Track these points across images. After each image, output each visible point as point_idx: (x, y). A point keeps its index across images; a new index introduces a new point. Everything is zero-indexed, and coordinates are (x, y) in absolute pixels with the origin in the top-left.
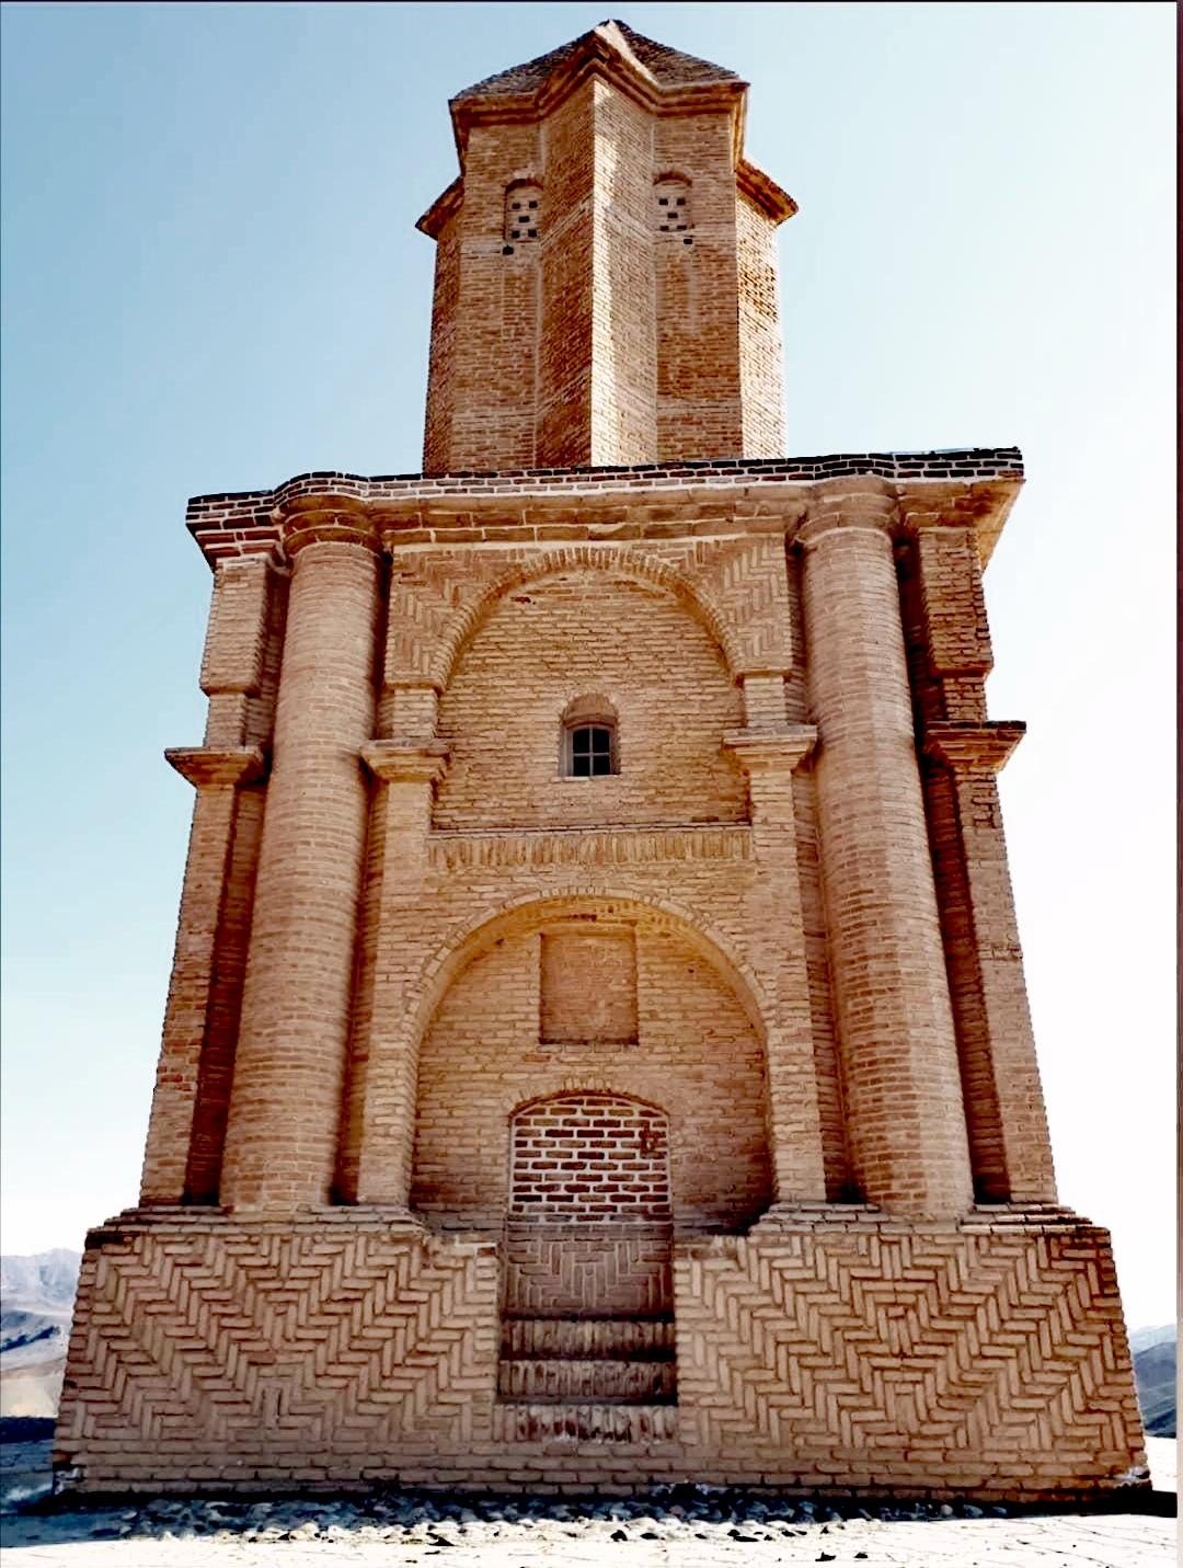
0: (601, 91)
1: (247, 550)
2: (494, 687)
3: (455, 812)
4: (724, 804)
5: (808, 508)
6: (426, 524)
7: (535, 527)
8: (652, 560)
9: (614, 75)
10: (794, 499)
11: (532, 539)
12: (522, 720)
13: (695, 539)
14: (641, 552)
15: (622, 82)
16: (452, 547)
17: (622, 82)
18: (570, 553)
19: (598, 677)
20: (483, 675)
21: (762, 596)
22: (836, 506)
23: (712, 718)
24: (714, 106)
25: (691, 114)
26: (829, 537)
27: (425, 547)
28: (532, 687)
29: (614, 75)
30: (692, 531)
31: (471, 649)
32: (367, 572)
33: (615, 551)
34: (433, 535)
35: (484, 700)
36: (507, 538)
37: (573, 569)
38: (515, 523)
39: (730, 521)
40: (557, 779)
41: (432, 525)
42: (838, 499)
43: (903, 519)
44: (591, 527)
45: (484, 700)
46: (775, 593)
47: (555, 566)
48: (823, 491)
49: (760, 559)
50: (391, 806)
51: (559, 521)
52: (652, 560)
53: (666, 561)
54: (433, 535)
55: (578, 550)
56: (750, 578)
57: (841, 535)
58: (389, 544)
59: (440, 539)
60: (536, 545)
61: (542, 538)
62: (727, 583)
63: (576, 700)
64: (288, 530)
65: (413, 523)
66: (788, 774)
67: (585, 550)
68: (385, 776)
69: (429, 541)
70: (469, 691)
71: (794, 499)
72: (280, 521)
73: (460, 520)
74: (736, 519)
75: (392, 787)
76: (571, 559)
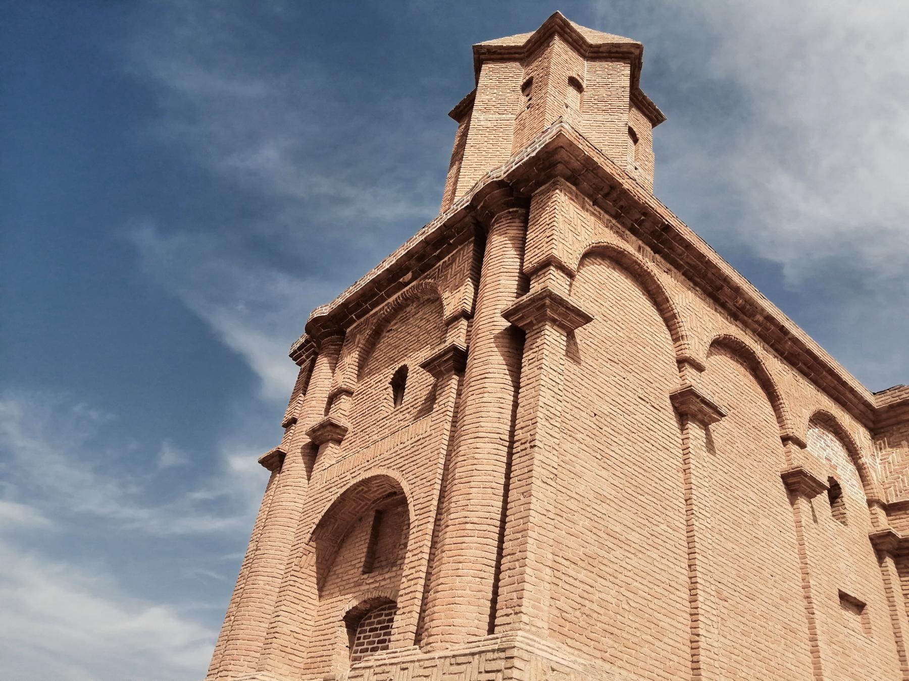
1: (307, 357)
5: (474, 218)
9: (493, 57)
10: (465, 217)
15: (500, 56)
17: (500, 56)
24: (547, 35)
25: (540, 46)
29: (493, 57)
30: (439, 258)
47: (399, 308)
48: (475, 204)
51: (389, 284)
59: (359, 317)
69: (355, 321)
71: (465, 217)
73: (359, 305)
76: (406, 299)
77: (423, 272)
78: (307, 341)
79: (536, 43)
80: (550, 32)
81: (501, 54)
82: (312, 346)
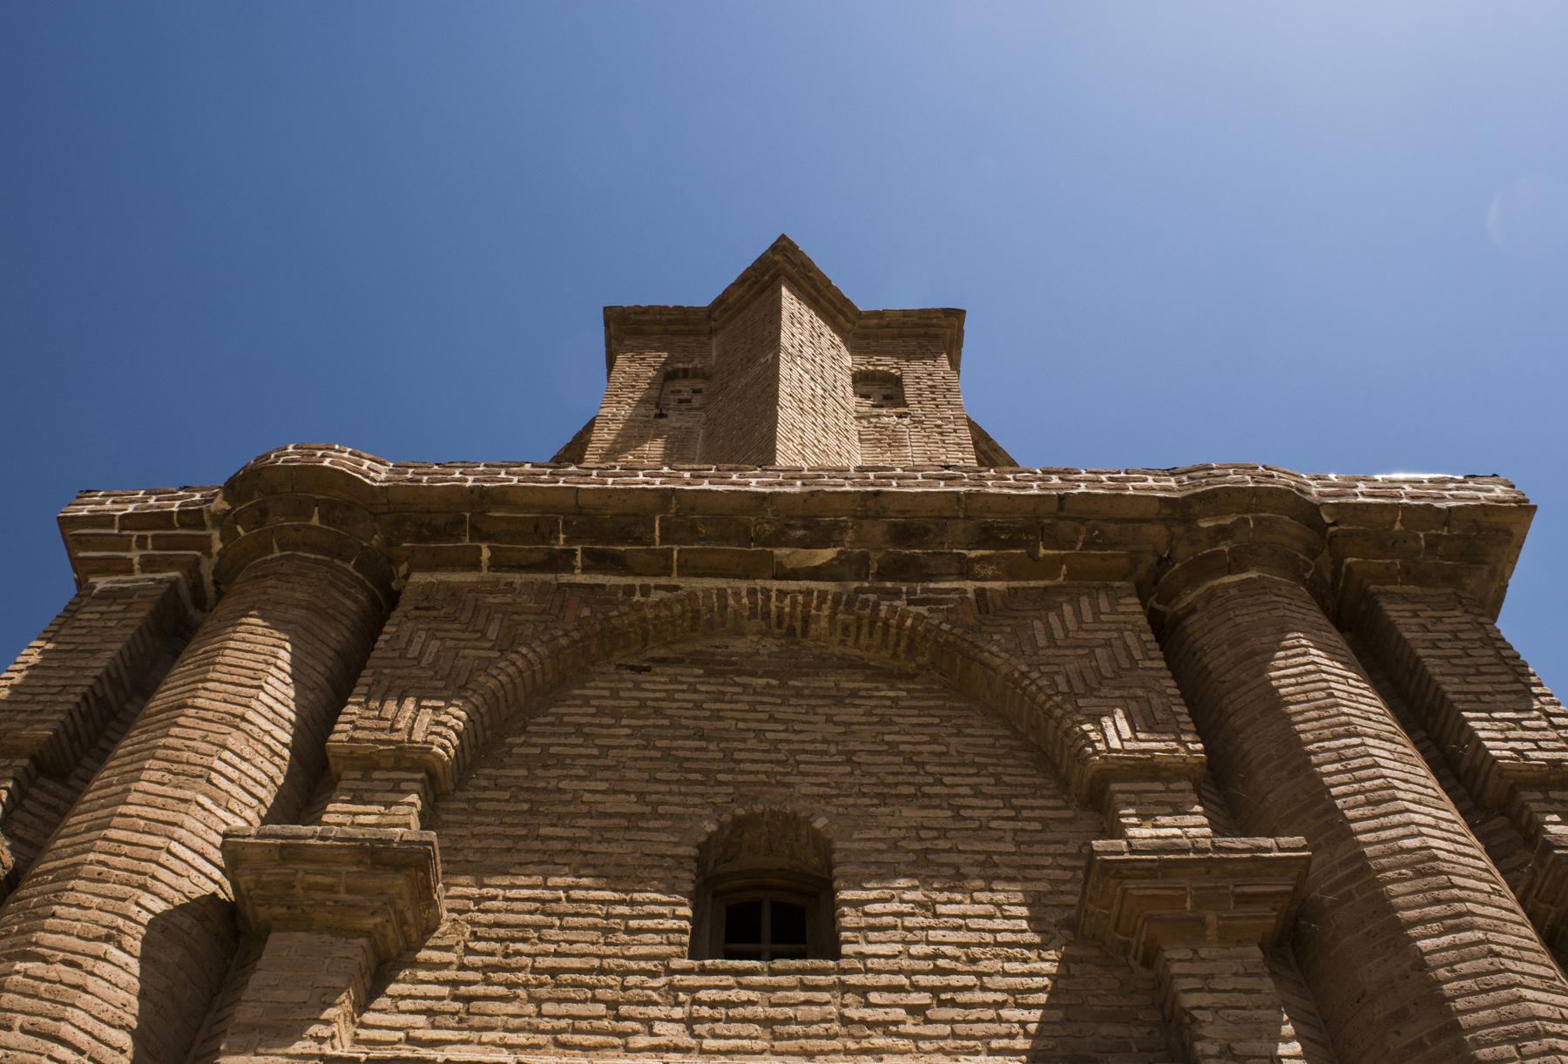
0: (789, 302)
1: (148, 564)
2: (560, 790)
3: (421, 1020)
4: (1106, 1029)
6: (479, 535)
7: (676, 548)
8: (893, 610)
11: (666, 571)
12: (614, 848)
13: (970, 586)
14: (872, 597)
15: (815, 294)
16: (517, 578)
18: (737, 594)
19: (788, 785)
20: (539, 772)
21: (1113, 658)
22: (1222, 532)
23: (1049, 861)
26: (1213, 589)
27: (470, 577)
28: (641, 795)
30: (965, 570)
31: (523, 731)
32: (352, 604)
33: (823, 595)
34: (486, 554)
35: (532, 812)
36: (617, 564)
37: (739, 632)
38: (639, 540)
39: (1033, 556)
40: (686, 963)
41: (483, 538)
42: (1228, 521)
43: (1336, 574)
44: (780, 552)
45: (532, 812)
46: (1138, 655)
48: (1197, 508)
49: (1097, 613)
50: (257, 979)
52: (893, 610)
53: (923, 610)
54: (486, 554)
55: (752, 592)
56: (1082, 635)
57: (1237, 585)
58: (403, 569)
59: (495, 565)
60: (675, 580)
61: (687, 570)
62: (1042, 641)
63: (738, 823)
64: (228, 535)
65: (452, 529)
66: (1256, 953)
67: (766, 592)
68: (263, 912)
69: (476, 566)
70: (507, 795)
72: (219, 519)
73: (540, 530)
74: (1042, 551)
75: (274, 940)
77: (882, 575)
78: (191, 517)
79: (888, 326)
80: (932, 331)
81: (818, 290)
82: (204, 545)
